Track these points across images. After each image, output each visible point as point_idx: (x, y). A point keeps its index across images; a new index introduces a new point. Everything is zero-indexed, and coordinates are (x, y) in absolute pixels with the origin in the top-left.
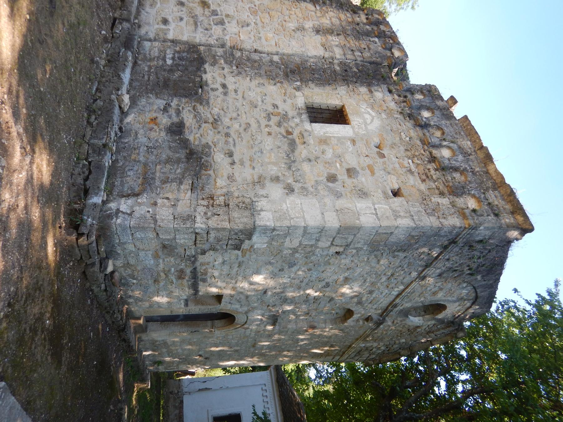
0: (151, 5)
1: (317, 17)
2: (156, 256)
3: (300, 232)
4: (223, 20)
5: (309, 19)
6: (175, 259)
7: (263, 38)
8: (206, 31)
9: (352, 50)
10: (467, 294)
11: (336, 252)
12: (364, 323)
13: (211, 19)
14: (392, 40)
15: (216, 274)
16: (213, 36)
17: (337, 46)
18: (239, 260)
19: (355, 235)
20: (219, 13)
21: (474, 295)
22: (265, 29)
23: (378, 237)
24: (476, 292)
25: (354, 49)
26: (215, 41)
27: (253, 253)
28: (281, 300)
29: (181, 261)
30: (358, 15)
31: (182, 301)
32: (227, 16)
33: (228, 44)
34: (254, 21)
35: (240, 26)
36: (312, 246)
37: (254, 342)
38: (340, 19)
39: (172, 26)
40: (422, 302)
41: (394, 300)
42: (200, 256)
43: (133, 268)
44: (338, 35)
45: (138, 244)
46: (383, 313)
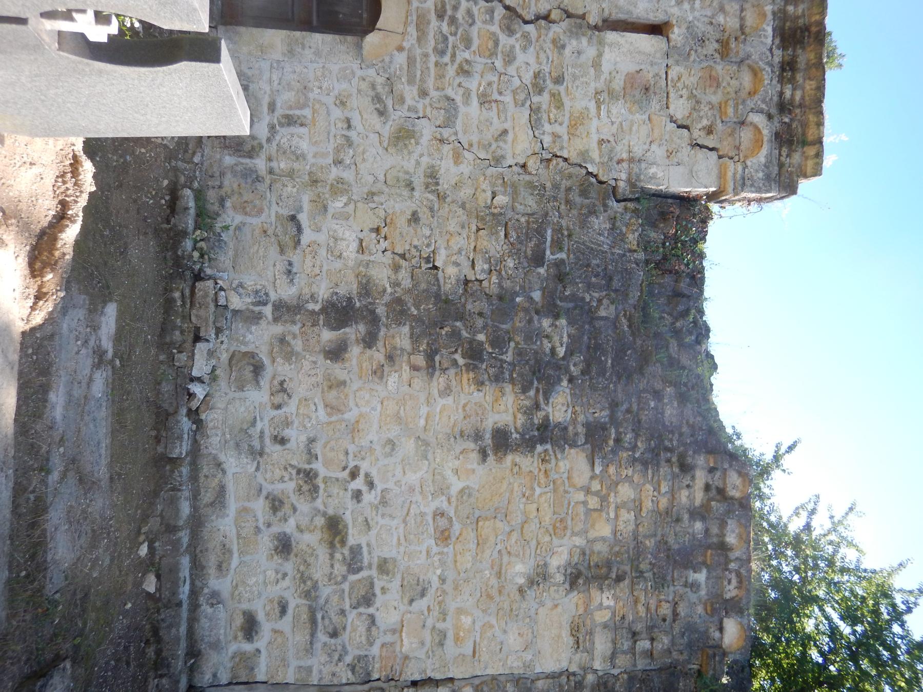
0: (219, 567)
1: (588, 512)
4: (372, 585)
5: (565, 528)
7: (450, 635)
8: (333, 641)
9: (634, 634)
13: (346, 586)
14: (739, 575)
16: (346, 653)
17: (605, 626)
20: (366, 562)
22: (458, 600)
25: (639, 627)
26: (350, 673)
30: (687, 481)
32: (384, 567)
33: (376, 676)
34: (439, 572)
35: (406, 601)
38: (638, 507)
39: (261, 642)
44: (619, 579)
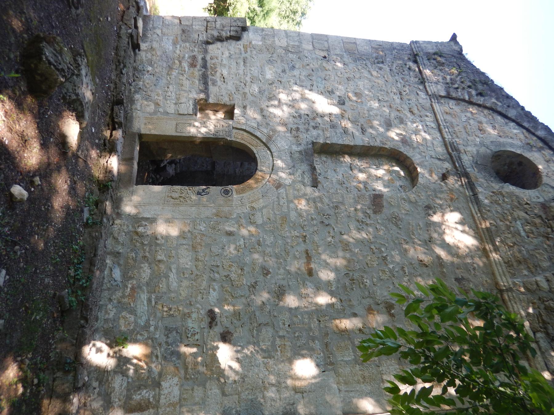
2: (175, 43)
3: (283, 34)
6: (190, 45)
10: (526, 137)
11: (325, 57)
12: (445, 183)
15: (225, 72)
18: (244, 55)
19: (327, 41)
21: (535, 138)
23: (347, 45)
24: (528, 130)
27: (253, 49)
28: (303, 120)
29: (195, 47)
31: (191, 102)
36: (298, 47)
37: (302, 247)
40: (482, 144)
41: (443, 138)
42: (210, 47)
43: (154, 53)
45: (164, 30)
46: (455, 167)
